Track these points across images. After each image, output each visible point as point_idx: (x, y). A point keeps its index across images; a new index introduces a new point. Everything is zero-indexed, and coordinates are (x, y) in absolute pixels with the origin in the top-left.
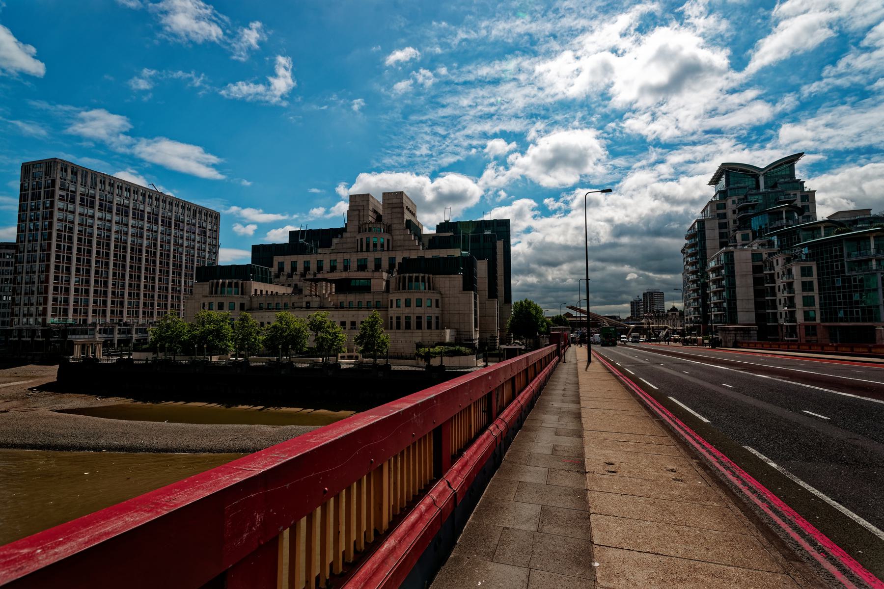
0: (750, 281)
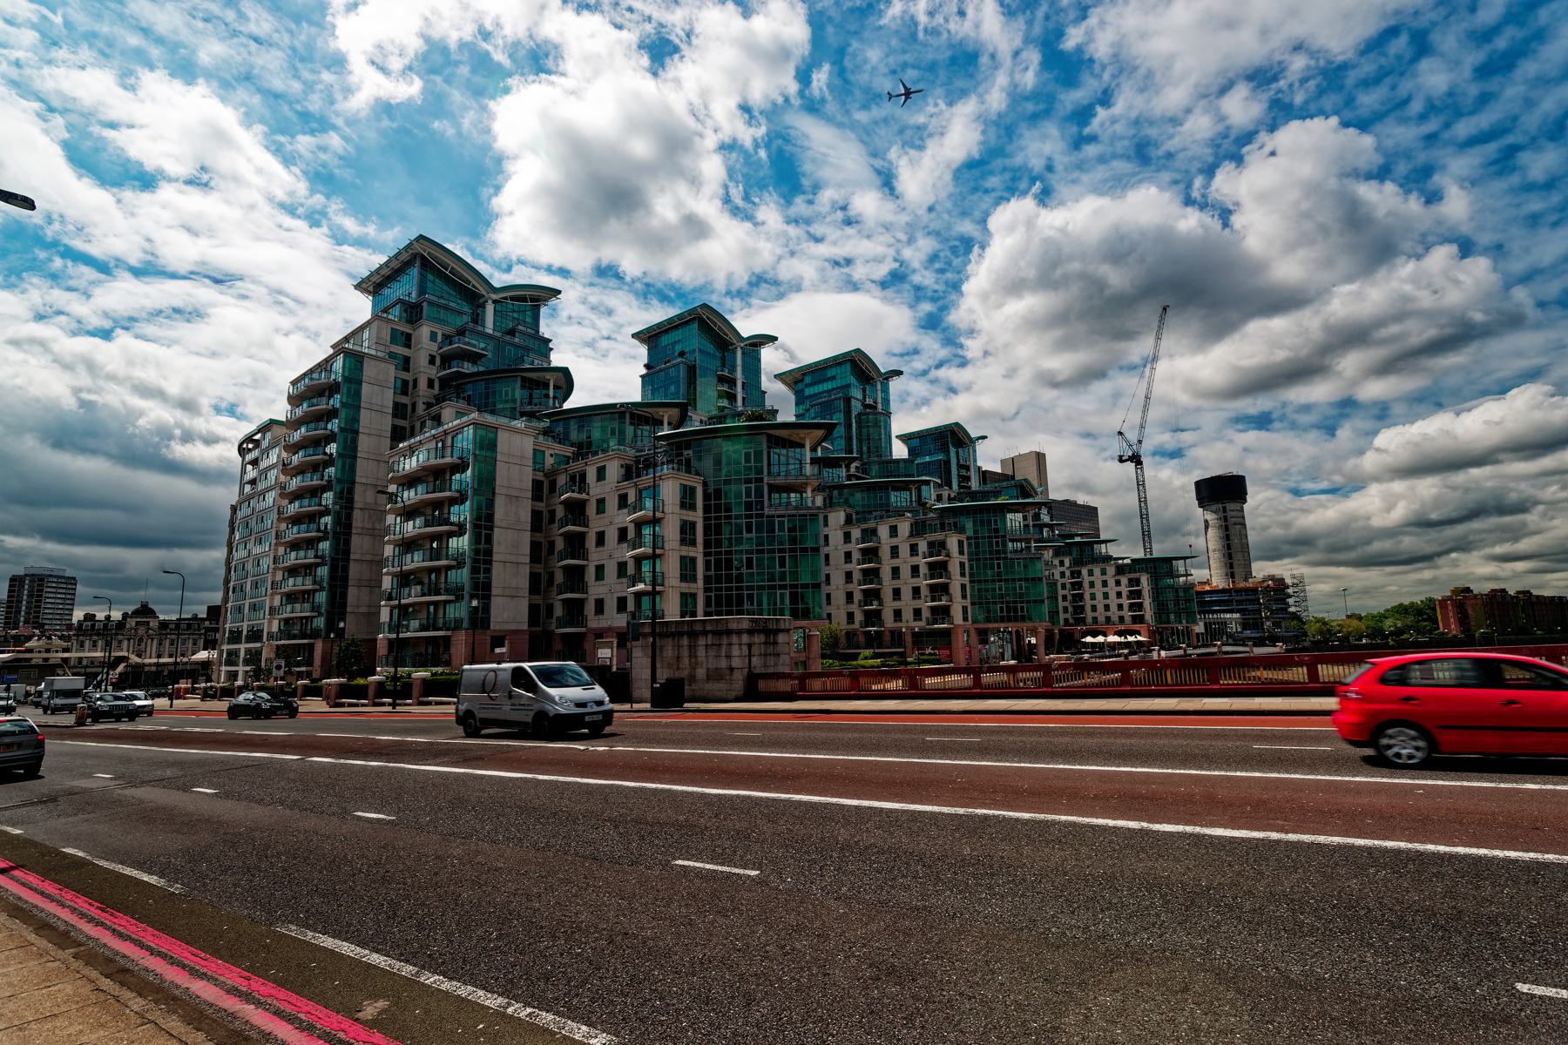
0: (526, 516)
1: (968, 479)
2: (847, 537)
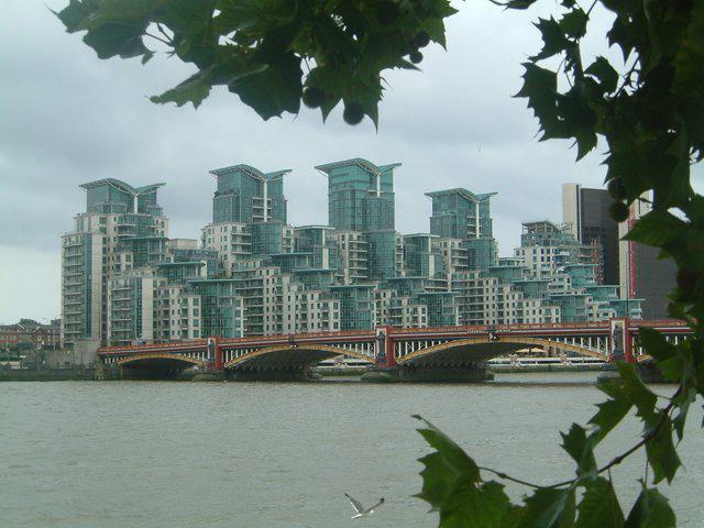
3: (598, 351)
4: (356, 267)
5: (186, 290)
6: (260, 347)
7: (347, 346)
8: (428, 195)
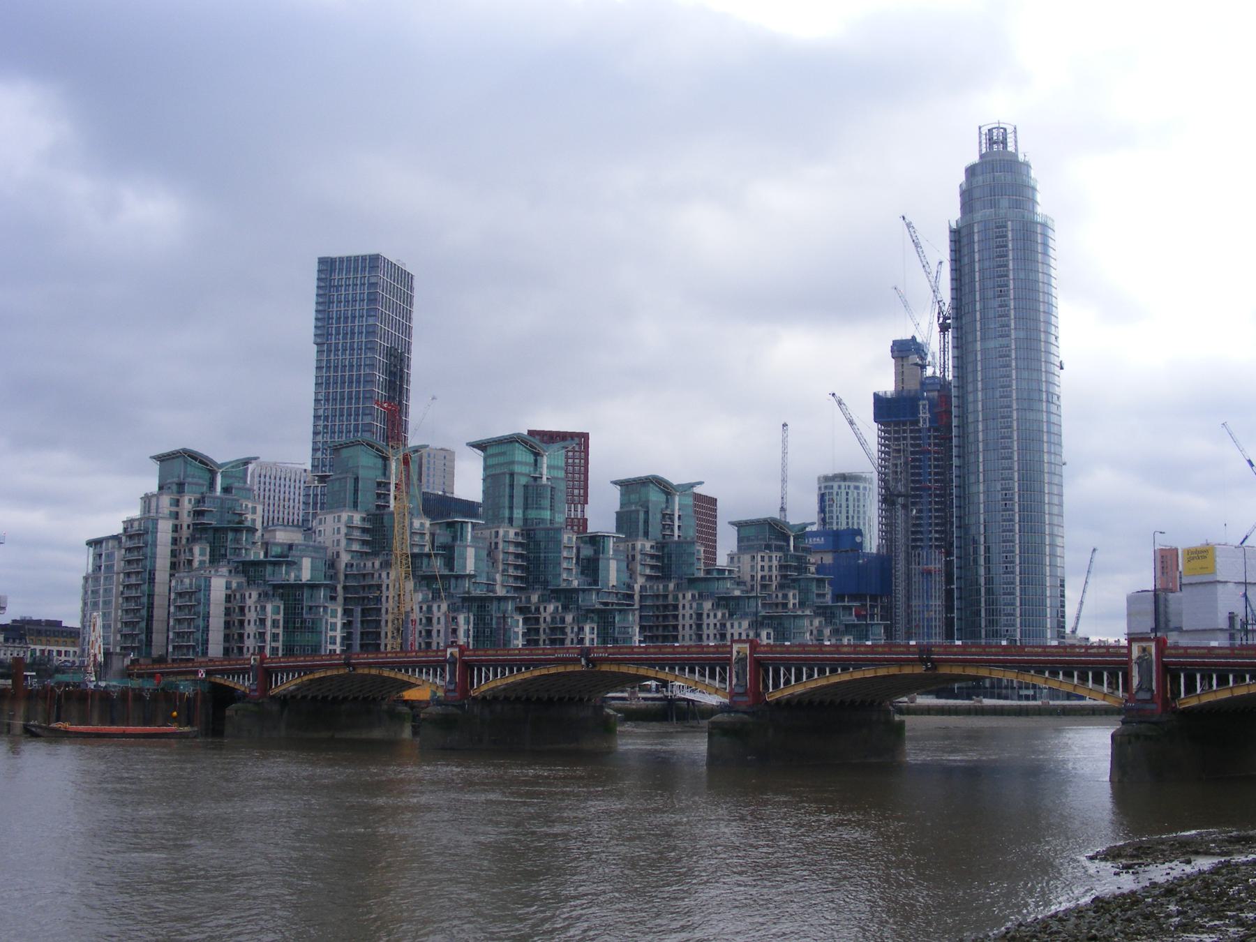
1: (671, 528)
2: (421, 608)
3: (717, 684)
4: (511, 571)
5: (266, 595)
6: (310, 669)
7: (414, 671)
8: (615, 483)
